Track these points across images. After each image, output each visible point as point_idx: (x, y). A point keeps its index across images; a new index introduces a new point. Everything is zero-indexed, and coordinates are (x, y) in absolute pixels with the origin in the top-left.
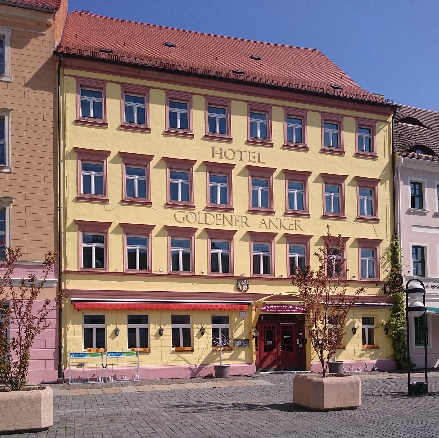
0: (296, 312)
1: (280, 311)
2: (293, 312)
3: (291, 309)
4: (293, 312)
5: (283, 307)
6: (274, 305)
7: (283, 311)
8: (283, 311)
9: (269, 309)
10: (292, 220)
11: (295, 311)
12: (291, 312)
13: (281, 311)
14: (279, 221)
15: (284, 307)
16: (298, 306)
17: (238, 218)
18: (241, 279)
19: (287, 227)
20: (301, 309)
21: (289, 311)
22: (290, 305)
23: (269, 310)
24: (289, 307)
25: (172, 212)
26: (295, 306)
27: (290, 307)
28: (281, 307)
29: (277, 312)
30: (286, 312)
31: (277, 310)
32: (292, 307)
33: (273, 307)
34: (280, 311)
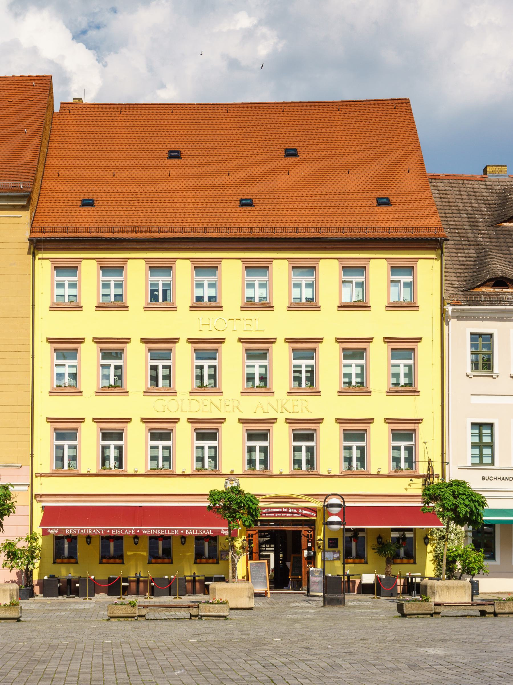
0: (299, 517)
1: (278, 515)
2: (296, 517)
3: (292, 513)
4: (296, 517)
5: (282, 510)
6: (271, 508)
7: (283, 515)
8: (283, 515)
9: (265, 513)
10: (299, 399)
11: (298, 515)
12: (293, 516)
13: (280, 515)
14: (279, 402)
15: (284, 510)
16: (302, 509)
17: (228, 403)
18: (231, 476)
19: (291, 410)
20: (306, 512)
21: (291, 515)
22: (293, 508)
23: (264, 515)
24: (290, 510)
25: (152, 400)
26: (297, 509)
27: (293, 511)
28: (281, 510)
29: (275, 516)
30: (286, 516)
31: (275, 515)
32: (295, 511)
33: (270, 510)
34: (278, 515)
